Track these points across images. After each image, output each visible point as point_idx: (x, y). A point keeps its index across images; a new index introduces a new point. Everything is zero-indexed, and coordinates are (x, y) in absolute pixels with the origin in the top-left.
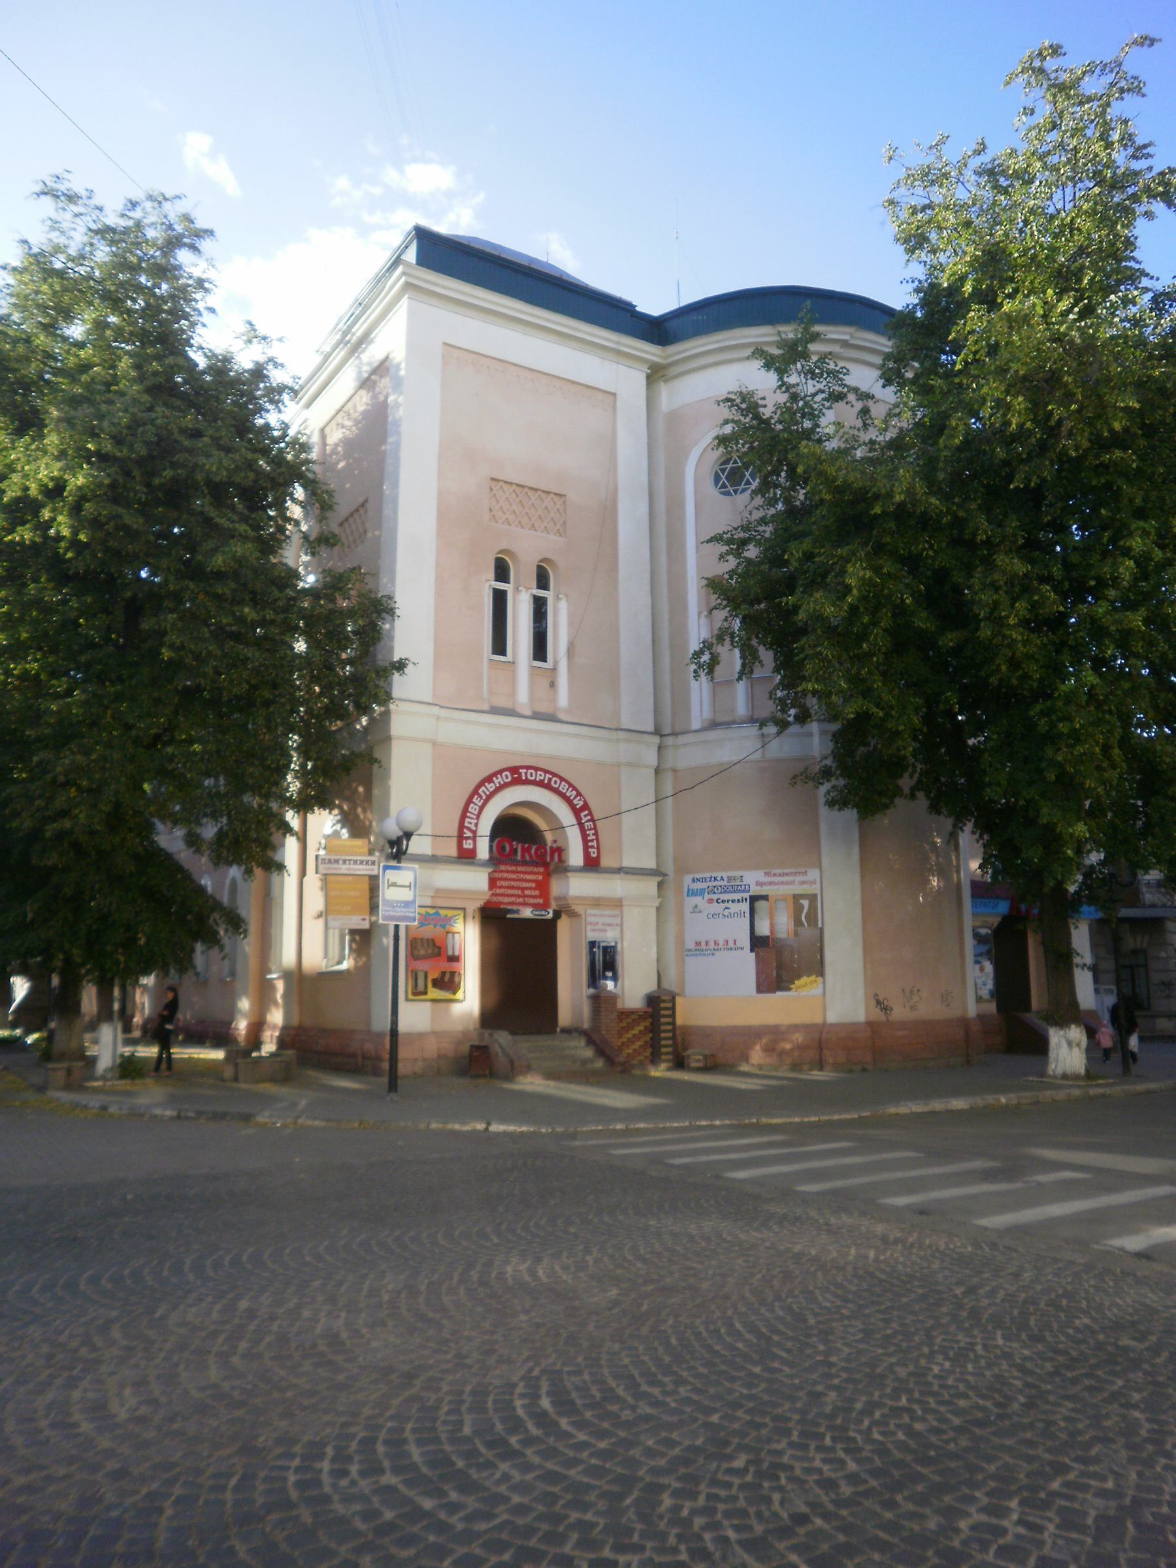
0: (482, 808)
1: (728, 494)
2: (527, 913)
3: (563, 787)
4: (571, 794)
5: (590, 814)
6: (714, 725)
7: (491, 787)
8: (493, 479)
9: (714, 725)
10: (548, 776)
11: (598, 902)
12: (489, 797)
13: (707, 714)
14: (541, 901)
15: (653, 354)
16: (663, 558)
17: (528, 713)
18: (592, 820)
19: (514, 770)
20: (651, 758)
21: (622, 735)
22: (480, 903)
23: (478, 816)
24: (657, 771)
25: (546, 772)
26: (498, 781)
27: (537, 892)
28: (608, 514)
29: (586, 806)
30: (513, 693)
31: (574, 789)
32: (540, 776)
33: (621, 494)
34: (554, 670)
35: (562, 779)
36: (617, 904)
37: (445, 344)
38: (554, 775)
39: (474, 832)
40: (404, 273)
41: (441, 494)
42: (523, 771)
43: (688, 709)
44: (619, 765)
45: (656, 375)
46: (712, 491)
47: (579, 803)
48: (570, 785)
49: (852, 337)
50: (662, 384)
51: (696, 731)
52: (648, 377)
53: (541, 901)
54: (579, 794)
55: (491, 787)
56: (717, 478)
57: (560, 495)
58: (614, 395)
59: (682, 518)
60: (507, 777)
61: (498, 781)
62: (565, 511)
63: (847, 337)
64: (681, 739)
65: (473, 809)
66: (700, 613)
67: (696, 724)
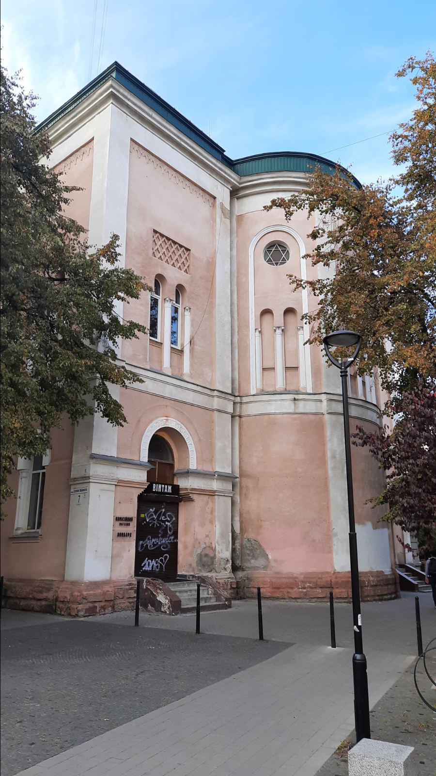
1: (272, 264)
6: (263, 393)
8: (155, 232)
9: (263, 393)
11: (202, 492)
13: (259, 386)
15: (234, 179)
16: (235, 296)
17: (170, 374)
20: (231, 410)
21: (216, 393)
24: (233, 417)
28: (211, 264)
30: (161, 362)
33: (218, 255)
34: (182, 351)
36: (212, 494)
40: (111, 86)
43: (248, 382)
44: (213, 410)
45: (235, 193)
50: (236, 199)
52: (231, 192)
57: (188, 250)
58: (215, 198)
64: (245, 399)
66: (256, 329)
67: (253, 392)
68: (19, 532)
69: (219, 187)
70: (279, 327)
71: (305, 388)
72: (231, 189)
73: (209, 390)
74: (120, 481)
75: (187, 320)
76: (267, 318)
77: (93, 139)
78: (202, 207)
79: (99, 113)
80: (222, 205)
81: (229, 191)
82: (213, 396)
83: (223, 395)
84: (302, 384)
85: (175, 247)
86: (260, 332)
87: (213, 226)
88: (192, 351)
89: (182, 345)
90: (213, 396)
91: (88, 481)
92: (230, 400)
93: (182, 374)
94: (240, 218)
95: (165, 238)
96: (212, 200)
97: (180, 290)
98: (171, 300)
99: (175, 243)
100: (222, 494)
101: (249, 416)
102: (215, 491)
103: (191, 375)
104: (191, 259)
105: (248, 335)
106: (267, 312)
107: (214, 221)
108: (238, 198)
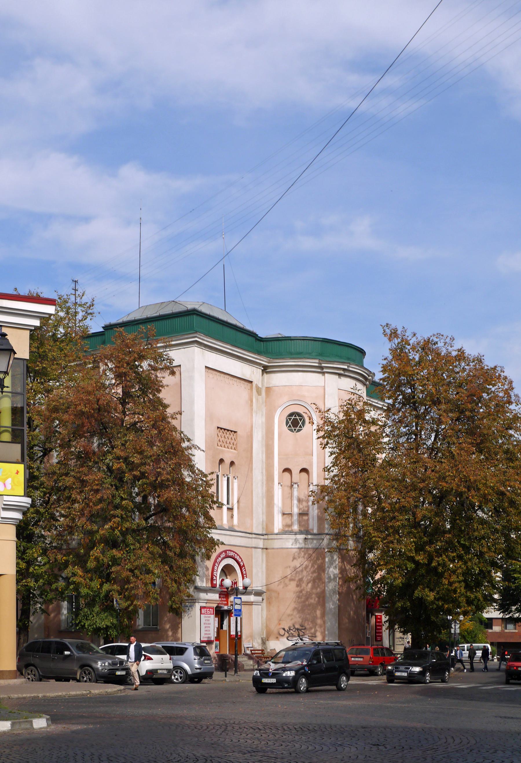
0: (218, 567)
1: (291, 430)
2: (226, 608)
3: (238, 558)
4: (240, 560)
5: (245, 568)
7: (220, 559)
8: (218, 428)
9: (283, 532)
10: (234, 553)
12: (220, 563)
14: (226, 602)
15: (265, 362)
17: (227, 528)
18: (245, 570)
19: (225, 551)
21: (254, 536)
22: (215, 605)
23: (217, 570)
25: (234, 552)
26: (222, 556)
27: (225, 599)
28: (250, 437)
29: (244, 565)
31: (241, 558)
32: (232, 554)
35: (238, 555)
37: (206, 367)
38: (236, 553)
39: (216, 577)
41: (206, 435)
42: (228, 552)
46: (285, 428)
47: (242, 564)
48: (240, 557)
49: (348, 367)
51: (277, 534)
53: (226, 602)
54: (242, 560)
55: (220, 559)
56: (287, 423)
57: (235, 432)
58: (251, 382)
59: (273, 439)
60: (223, 556)
61: (222, 556)
62: (237, 439)
63: (346, 367)
64: (270, 537)
65: (216, 568)
66: (279, 483)
67: (276, 531)
68: (140, 627)
69: (255, 372)
70: (296, 483)
71: (313, 530)
72: (263, 368)
73: (249, 534)
74: (208, 600)
75: (235, 485)
76: (287, 474)
77: (180, 366)
78: (242, 389)
79: (184, 348)
80: (256, 385)
81: (261, 370)
82: (251, 538)
83: (258, 536)
84: (311, 527)
85: (228, 433)
86: (281, 486)
87: (251, 405)
88: (238, 508)
89: (233, 504)
90: (251, 538)
91: (195, 601)
92: (260, 539)
93: (233, 525)
94: (268, 389)
95: (223, 430)
96: (249, 384)
97: (232, 463)
98: (227, 475)
99: (228, 430)
100: (257, 603)
101: (273, 549)
102: (252, 602)
103: (238, 526)
104: (238, 439)
105: (273, 488)
106: (287, 470)
107: (252, 401)
108: (267, 373)
